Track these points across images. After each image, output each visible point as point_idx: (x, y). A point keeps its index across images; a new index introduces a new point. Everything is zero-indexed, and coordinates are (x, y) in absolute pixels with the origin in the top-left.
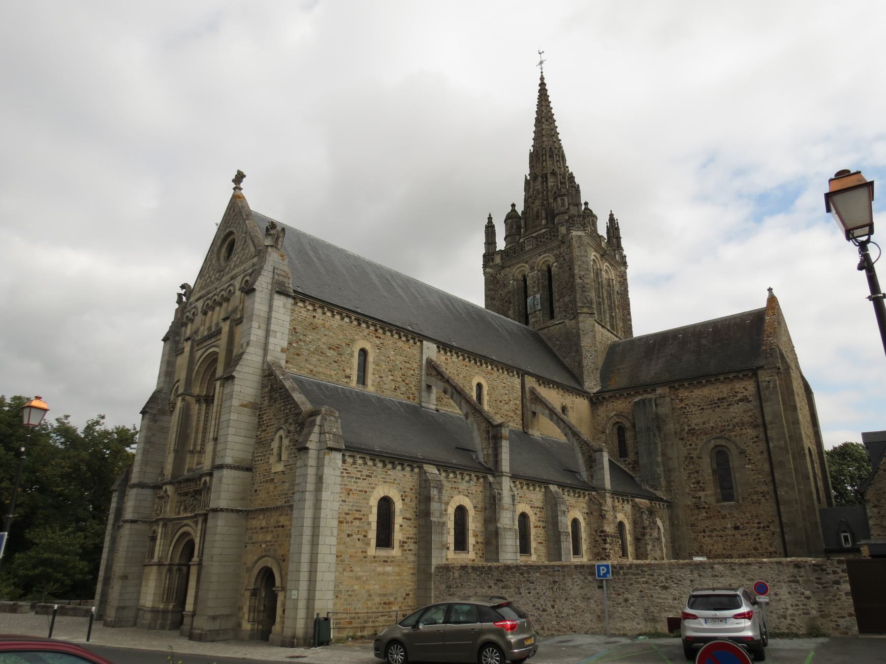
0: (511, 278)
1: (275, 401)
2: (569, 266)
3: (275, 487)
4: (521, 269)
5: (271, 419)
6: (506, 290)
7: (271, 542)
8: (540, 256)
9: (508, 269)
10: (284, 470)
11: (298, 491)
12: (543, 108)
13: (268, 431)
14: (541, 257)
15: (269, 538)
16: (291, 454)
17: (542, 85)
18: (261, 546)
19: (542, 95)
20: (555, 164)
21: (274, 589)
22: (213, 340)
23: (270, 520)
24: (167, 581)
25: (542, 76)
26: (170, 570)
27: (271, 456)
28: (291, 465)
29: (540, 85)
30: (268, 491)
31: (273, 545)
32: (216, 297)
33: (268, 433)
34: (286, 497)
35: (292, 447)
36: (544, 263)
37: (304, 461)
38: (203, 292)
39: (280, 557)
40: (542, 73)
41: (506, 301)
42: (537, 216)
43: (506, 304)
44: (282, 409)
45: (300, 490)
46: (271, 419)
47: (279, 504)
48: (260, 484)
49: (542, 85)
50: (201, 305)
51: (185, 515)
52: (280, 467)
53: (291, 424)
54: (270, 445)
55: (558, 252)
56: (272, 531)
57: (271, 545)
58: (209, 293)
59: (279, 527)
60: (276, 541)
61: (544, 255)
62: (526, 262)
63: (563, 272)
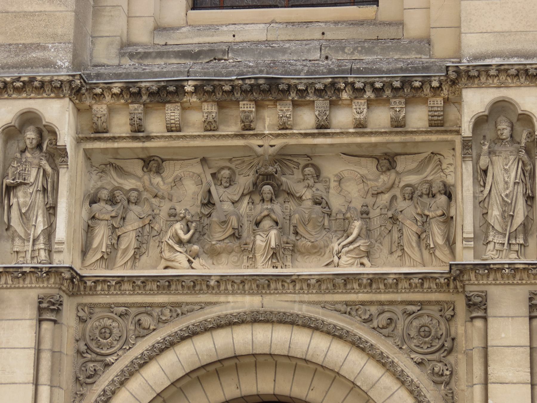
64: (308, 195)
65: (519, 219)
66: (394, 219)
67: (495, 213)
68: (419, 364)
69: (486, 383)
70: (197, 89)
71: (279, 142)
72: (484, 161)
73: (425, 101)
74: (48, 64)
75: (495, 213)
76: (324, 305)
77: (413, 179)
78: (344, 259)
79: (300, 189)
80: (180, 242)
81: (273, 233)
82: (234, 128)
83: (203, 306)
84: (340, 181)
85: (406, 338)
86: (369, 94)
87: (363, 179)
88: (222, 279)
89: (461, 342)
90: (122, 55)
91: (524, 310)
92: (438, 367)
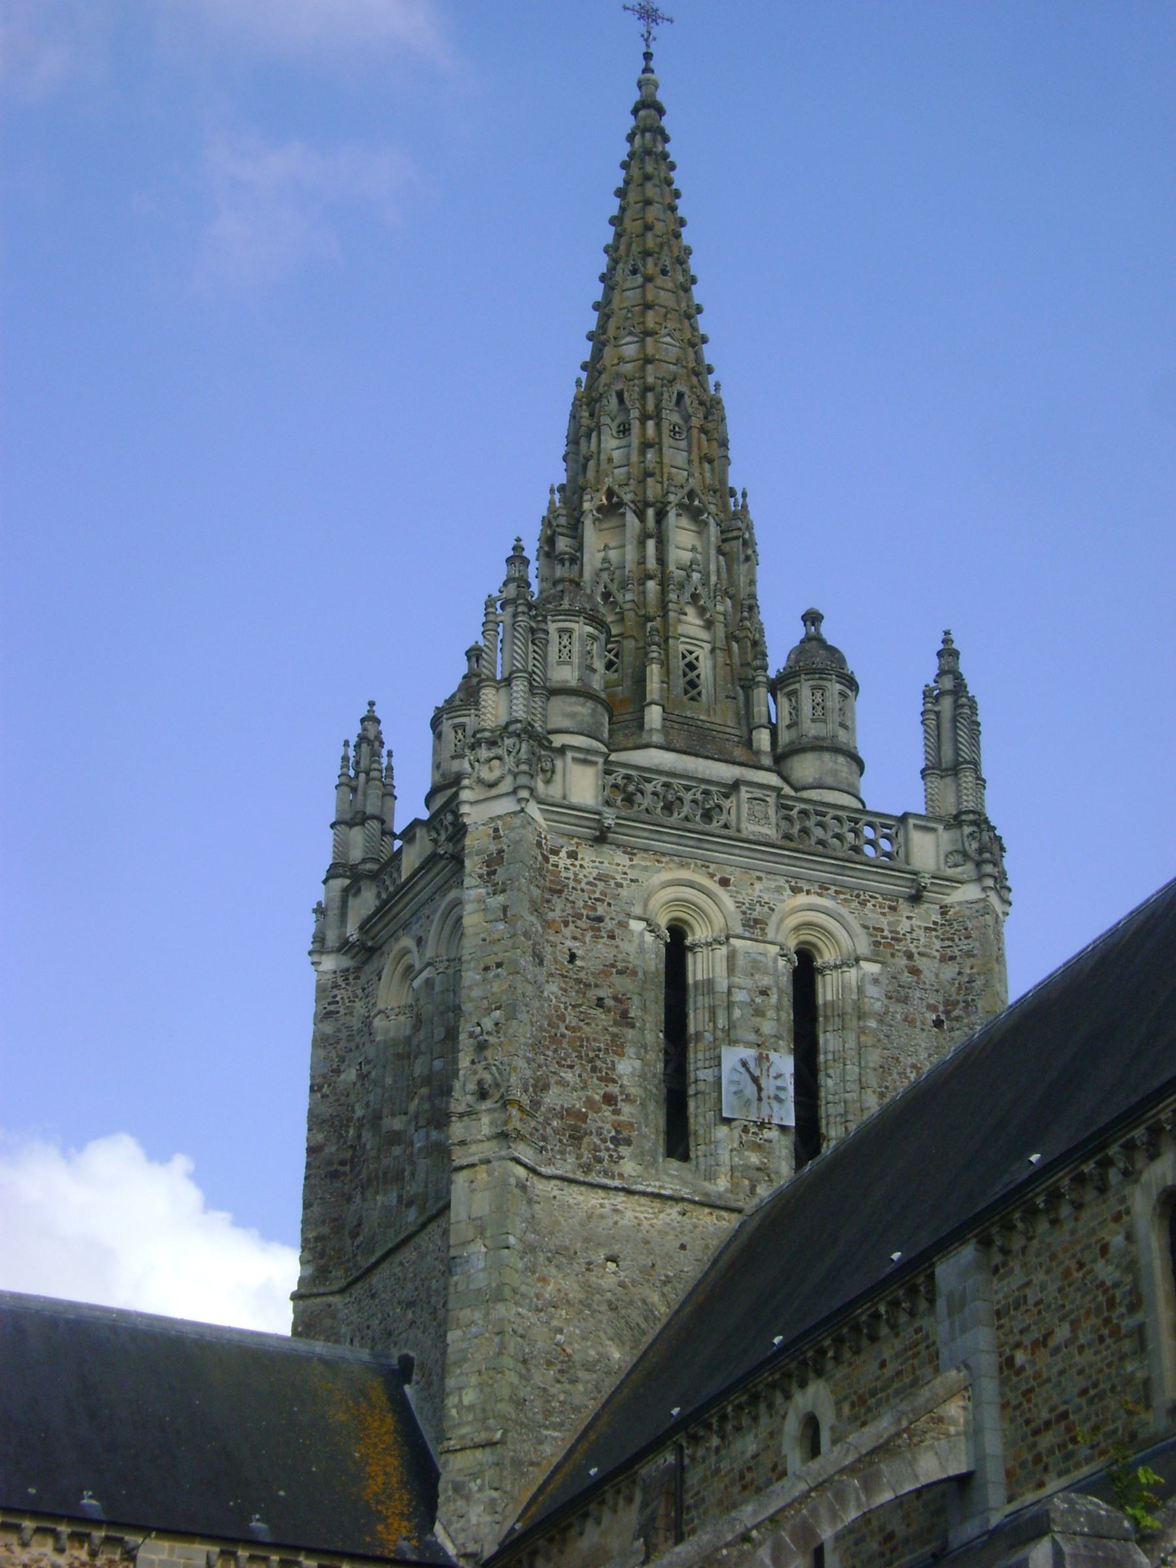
0: (637, 910)
2: (932, 1008)
4: (689, 893)
6: (603, 951)
8: (796, 890)
9: (621, 858)
12: (653, 212)
14: (802, 899)
36: (797, 928)
40: (648, 56)
41: (600, 1002)
42: (693, 684)
55: (884, 922)
61: (814, 899)
62: (724, 882)
63: (909, 1020)
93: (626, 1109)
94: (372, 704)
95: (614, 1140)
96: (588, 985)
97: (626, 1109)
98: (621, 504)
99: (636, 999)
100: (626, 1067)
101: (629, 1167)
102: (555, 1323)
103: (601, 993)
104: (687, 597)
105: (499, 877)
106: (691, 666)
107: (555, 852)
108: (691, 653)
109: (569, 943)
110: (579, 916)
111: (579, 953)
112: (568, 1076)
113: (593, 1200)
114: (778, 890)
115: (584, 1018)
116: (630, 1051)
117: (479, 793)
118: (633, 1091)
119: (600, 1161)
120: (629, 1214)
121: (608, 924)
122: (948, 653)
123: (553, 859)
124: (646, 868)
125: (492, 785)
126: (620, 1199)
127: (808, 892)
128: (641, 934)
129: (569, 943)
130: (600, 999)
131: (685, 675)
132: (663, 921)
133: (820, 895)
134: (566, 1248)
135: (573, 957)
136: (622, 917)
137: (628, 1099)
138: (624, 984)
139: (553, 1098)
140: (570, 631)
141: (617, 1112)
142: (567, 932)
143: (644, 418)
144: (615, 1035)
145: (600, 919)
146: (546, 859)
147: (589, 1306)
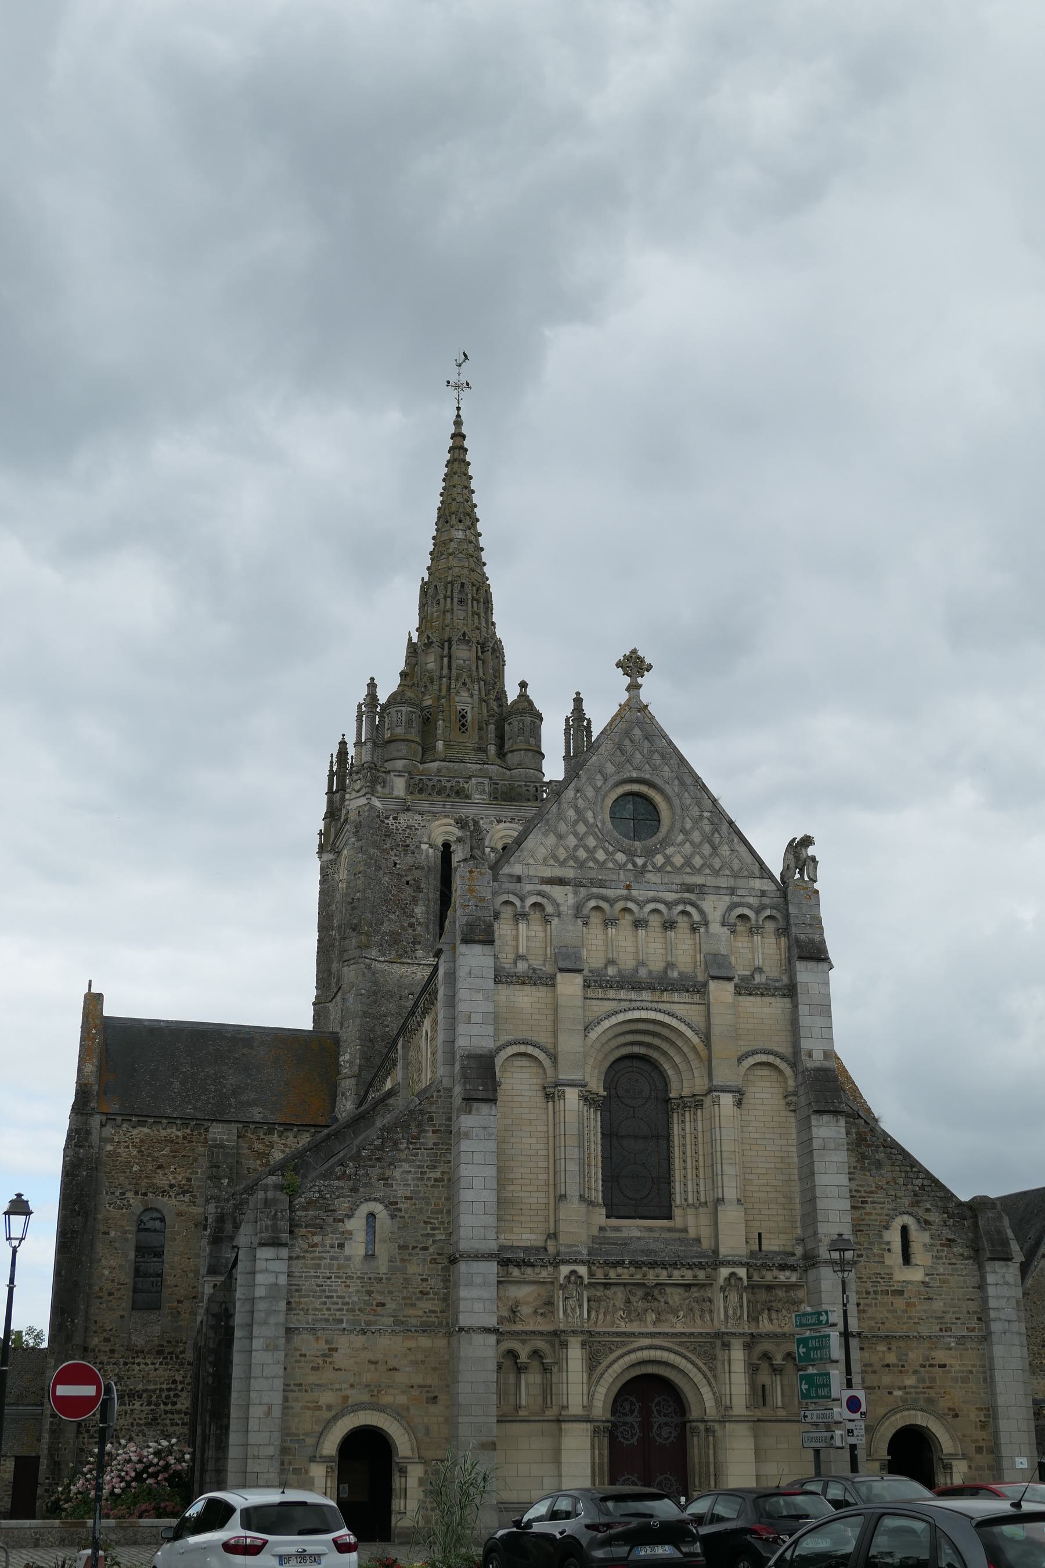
0: (425, 839)
1: (879, 1165)
3: (908, 1305)
5: (872, 1192)
6: (410, 860)
7: (916, 1387)
8: (499, 822)
9: (418, 817)
10: (927, 1279)
11: (1000, 1319)
13: (868, 1210)
14: (502, 825)
15: (910, 1381)
16: (937, 1258)
17: (458, 436)
18: (890, 1393)
19: (455, 460)
20: (470, 620)
21: (890, 1457)
22: (645, 995)
23: (907, 1355)
24: (597, 1452)
25: (458, 416)
26: (595, 1432)
27: (886, 1254)
28: (944, 1274)
29: (453, 436)
30: (891, 1308)
31: (924, 1393)
32: (631, 905)
33: (871, 1214)
34: (941, 1323)
35: (940, 1248)
36: (501, 838)
37: (1004, 1277)
38: (569, 873)
39: (946, 1411)
40: (458, 409)
42: (463, 725)
43: (409, 890)
44: (901, 1181)
45: (1003, 1317)
46: (872, 1192)
47: (925, 1331)
48: (864, 1295)
49: (458, 436)
50: (571, 900)
51: (634, 1327)
52: (916, 1275)
53: (928, 1210)
54: (881, 1236)
56: (915, 1372)
57: (917, 1393)
58: (602, 884)
59: (931, 1366)
60: (931, 1388)
61: (508, 825)
64: (662, 1300)
65: (739, 1314)
66: (691, 1310)
67: (730, 1312)
68: (705, 1364)
69: (730, 1372)
70: (630, 1263)
71: (655, 1282)
72: (726, 1293)
73: (705, 1269)
74: (579, 1253)
75: (730, 1312)
76: (672, 1342)
77: (696, 1295)
78: (678, 1325)
79: (659, 1297)
80: (622, 1317)
81: (654, 1316)
82: (638, 1277)
83: (632, 1342)
84: (672, 1294)
85: (699, 1355)
86: (687, 1266)
87: (680, 1294)
88: (640, 1333)
89: (719, 1357)
90: (593, 1243)
91: (742, 1347)
92: (711, 1365)
93: (419, 928)
94: (343, 735)
95: (414, 943)
96: (402, 876)
97: (419, 928)
98: (432, 642)
99: (424, 880)
100: (419, 910)
101: (420, 953)
102: (385, 1023)
103: (408, 878)
104: (460, 683)
105: (360, 833)
106: (463, 717)
107: (388, 818)
108: (463, 710)
109: (393, 858)
110: (398, 846)
111: (398, 862)
112: (393, 917)
113: (404, 969)
114: (491, 822)
115: (401, 891)
116: (420, 903)
117: (354, 795)
118: (422, 920)
119: (406, 952)
120: (419, 974)
121: (412, 848)
122: (578, 701)
123: (386, 821)
124: (429, 820)
125: (358, 791)
126: (414, 968)
127: (505, 822)
128: (427, 850)
129: (393, 858)
130: (408, 883)
131: (460, 721)
132: (439, 842)
133: (510, 822)
134: (391, 991)
135: (395, 864)
136: (418, 844)
137: (420, 924)
138: (418, 874)
139: (385, 927)
140: (401, 711)
141: (414, 930)
142: (392, 853)
143: (445, 598)
144: (414, 897)
145: (408, 846)
146: (383, 822)
147: (400, 1015)
